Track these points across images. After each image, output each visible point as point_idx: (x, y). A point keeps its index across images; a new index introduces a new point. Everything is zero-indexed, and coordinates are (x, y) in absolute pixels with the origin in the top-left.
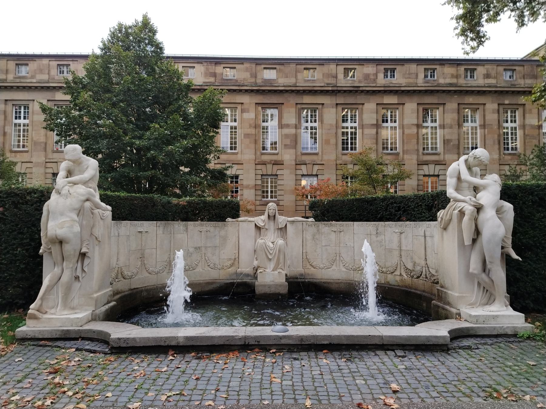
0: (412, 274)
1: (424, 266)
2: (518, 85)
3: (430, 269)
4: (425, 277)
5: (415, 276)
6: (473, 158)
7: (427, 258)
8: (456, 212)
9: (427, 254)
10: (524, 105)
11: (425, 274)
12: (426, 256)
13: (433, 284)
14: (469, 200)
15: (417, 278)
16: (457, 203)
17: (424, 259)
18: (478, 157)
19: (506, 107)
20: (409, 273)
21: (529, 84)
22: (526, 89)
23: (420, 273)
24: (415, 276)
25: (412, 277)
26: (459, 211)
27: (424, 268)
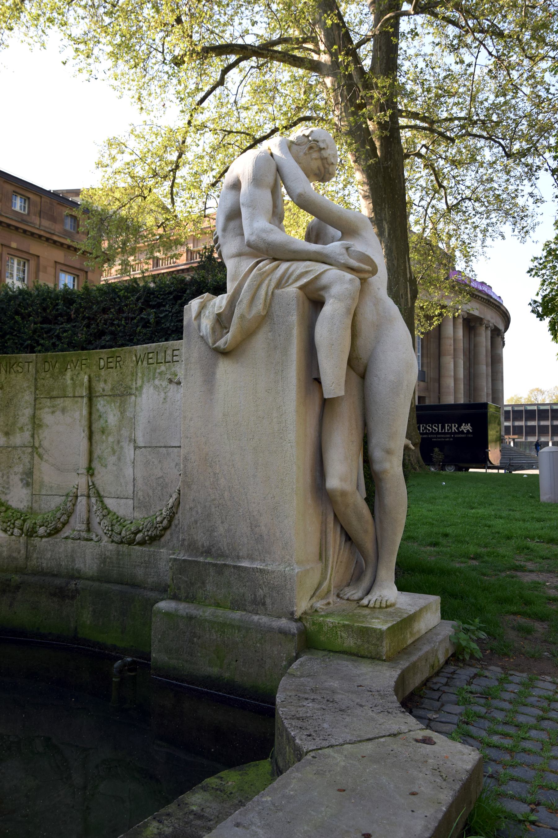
0: (27, 525)
1: (83, 490)
2: (31, 223)
3: (110, 503)
4: (84, 527)
5: (42, 531)
6: (305, 148)
7: (96, 464)
8: (292, 290)
9: (97, 452)
10: (38, 257)
11: (85, 516)
12: (91, 461)
13: (124, 548)
14: (344, 251)
15: (49, 535)
16: (284, 266)
17: (85, 471)
18: (322, 145)
19: (12, 252)
20: (18, 523)
21: (45, 227)
22: (42, 233)
23: (65, 517)
24: (42, 531)
25: (31, 533)
26: (301, 288)
27: (82, 501)
